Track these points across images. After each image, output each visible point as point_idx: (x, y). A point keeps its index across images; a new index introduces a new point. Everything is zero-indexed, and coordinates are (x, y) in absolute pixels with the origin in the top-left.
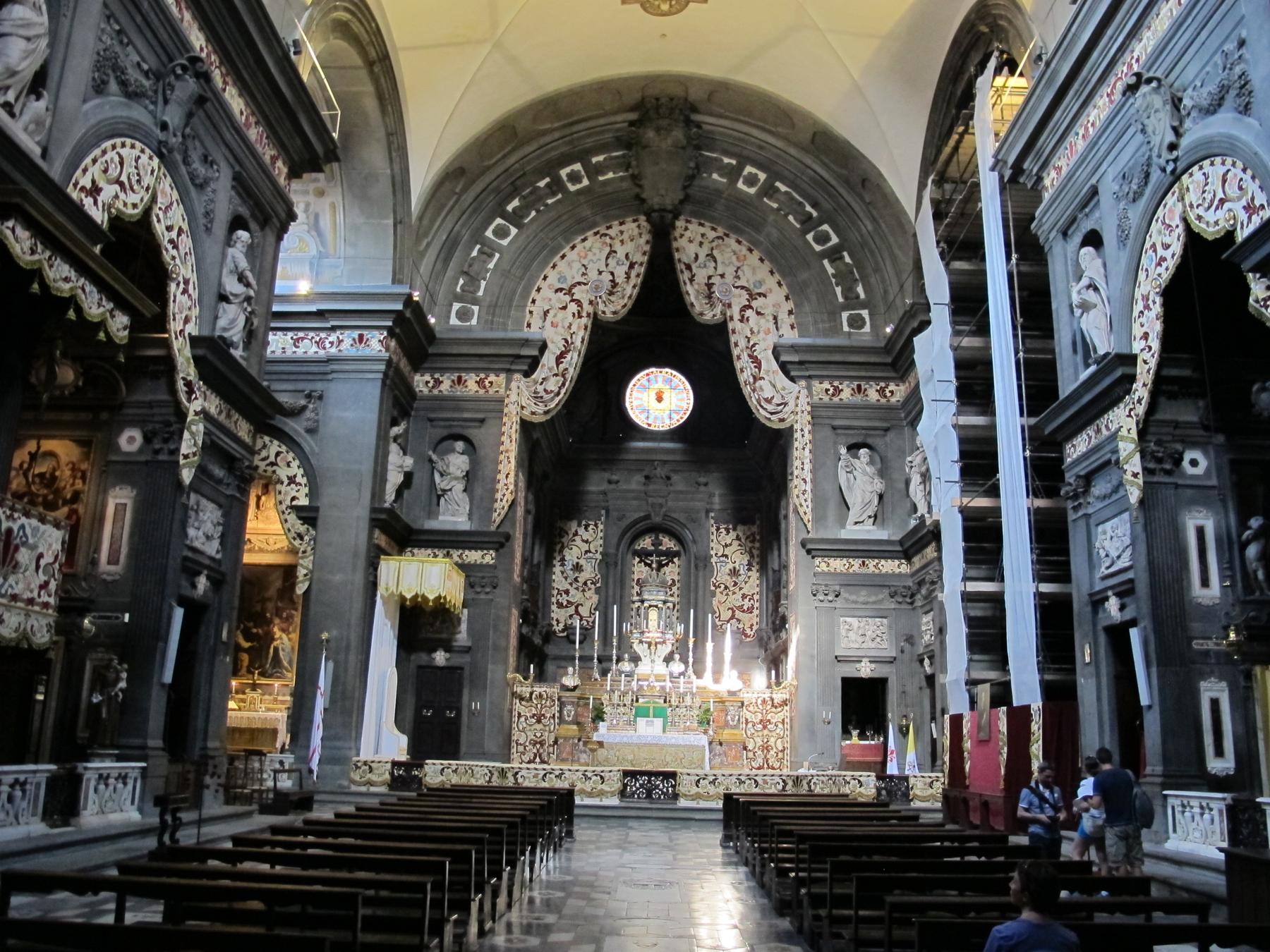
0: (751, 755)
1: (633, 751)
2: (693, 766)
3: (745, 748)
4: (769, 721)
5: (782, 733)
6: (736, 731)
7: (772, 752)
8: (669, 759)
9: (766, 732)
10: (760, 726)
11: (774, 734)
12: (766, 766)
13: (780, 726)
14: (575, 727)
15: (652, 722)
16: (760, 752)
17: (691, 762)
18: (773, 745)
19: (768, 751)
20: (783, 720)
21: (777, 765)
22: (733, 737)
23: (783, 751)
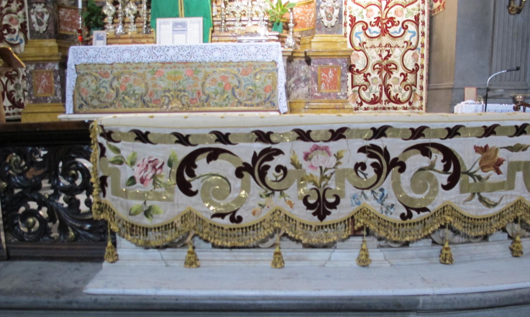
0: (359, 79)
1: (143, 76)
2: (257, 100)
3: (350, 68)
4: (391, 20)
5: (414, 41)
6: (334, 38)
7: (396, 74)
8: (210, 88)
9: (386, 40)
10: (377, 29)
11: (400, 42)
12: (384, 97)
13: (412, 27)
14: (52, 43)
15: (184, 25)
16: (375, 75)
17: (253, 94)
18: (398, 61)
19: (390, 72)
20: (417, 18)
21: (404, 95)
22: (330, 47)
23: (414, 71)
